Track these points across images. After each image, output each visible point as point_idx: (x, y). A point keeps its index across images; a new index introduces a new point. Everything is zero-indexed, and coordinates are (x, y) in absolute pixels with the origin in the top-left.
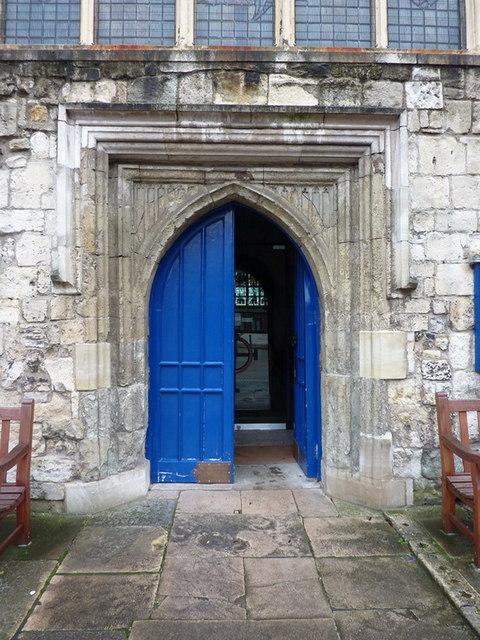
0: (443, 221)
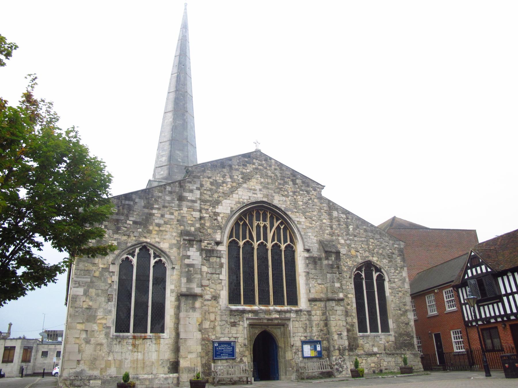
0: (297, 334)
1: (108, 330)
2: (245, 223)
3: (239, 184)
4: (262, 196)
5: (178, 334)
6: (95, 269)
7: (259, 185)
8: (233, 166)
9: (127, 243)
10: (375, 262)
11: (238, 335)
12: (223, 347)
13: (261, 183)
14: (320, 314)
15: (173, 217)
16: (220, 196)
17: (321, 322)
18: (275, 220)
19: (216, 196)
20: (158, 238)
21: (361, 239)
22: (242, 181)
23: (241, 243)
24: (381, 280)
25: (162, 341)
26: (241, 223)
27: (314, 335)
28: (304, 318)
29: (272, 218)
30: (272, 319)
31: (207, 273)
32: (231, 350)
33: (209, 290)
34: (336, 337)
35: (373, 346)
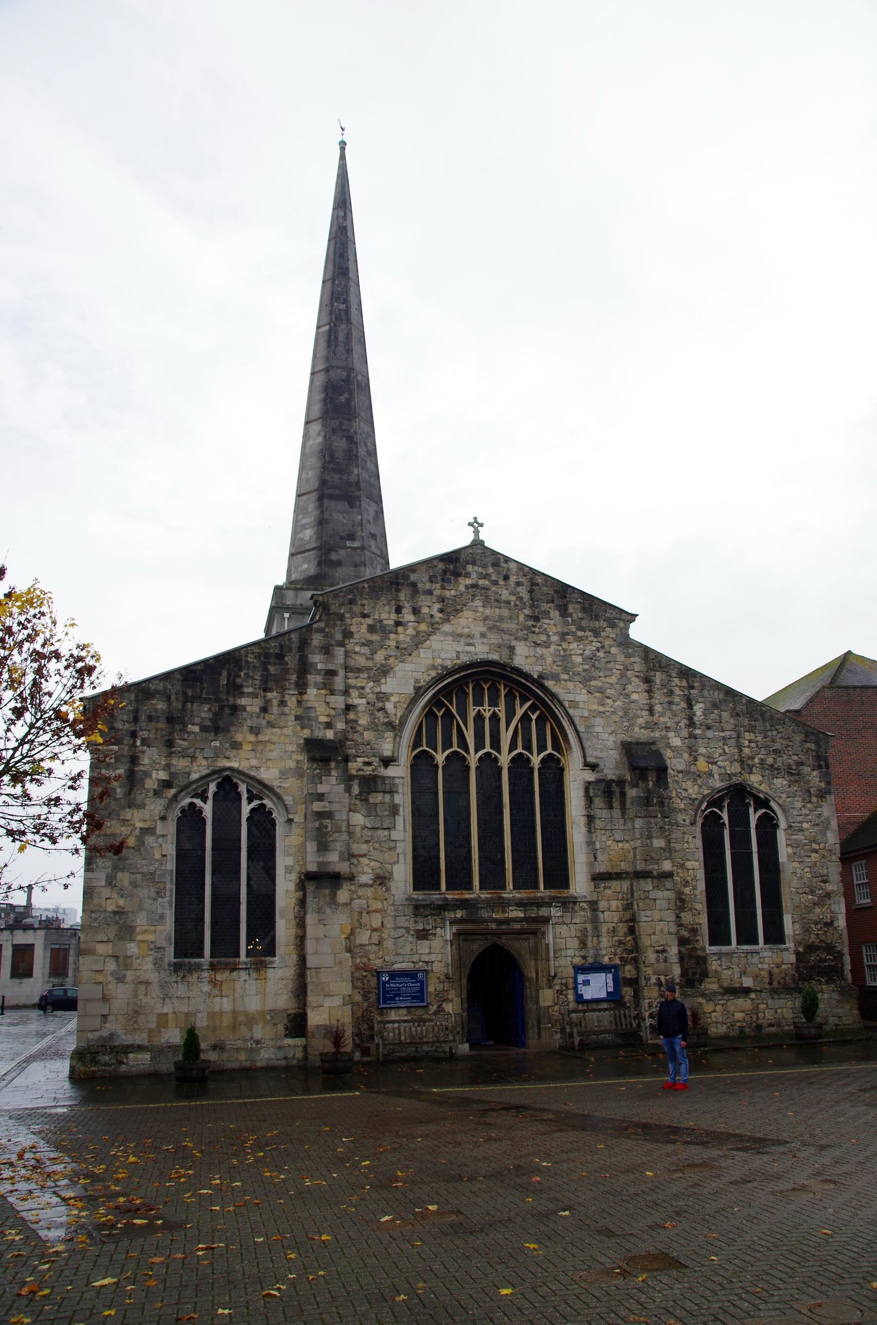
1: (159, 955)
2: (448, 712)
3: (433, 624)
4: (486, 649)
5: (302, 960)
6: (126, 832)
7: (481, 623)
8: (420, 585)
9: (189, 774)
10: (756, 785)
11: (433, 958)
12: (401, 983)
13: (486, 619)
14: (617, 907)
16: (390, 656)
17: (621, 925)
18: (518, 702)
19: (380, 657)
20: (256, 758)
21: (722, 734)
22: (441, 618)
23: (440, 758)
24: (768, 825)
25: (270, 973)
26: (440, 714)
27: (604, 952)
28: (581, 916)
29: (510, 697)
30: (508, 921)
31: (364, 827)
33: (368, 865)
34: (651, 957)
35: (744, 973)
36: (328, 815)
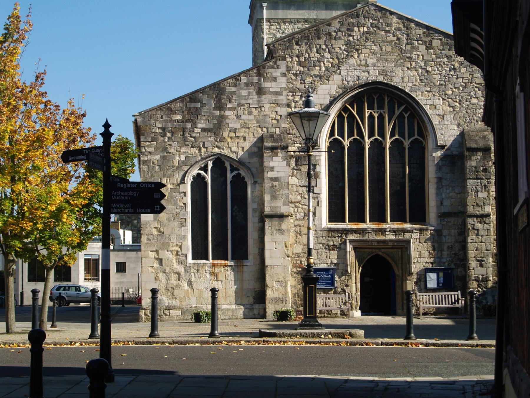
12: (320, 275)
15: (251, 117)
17: (456, 244)
18: (396, 106)
25: (245, 269)
27: (445, 260)
32: (330, 279)
34: (473, 263)
36: (276, 179)
